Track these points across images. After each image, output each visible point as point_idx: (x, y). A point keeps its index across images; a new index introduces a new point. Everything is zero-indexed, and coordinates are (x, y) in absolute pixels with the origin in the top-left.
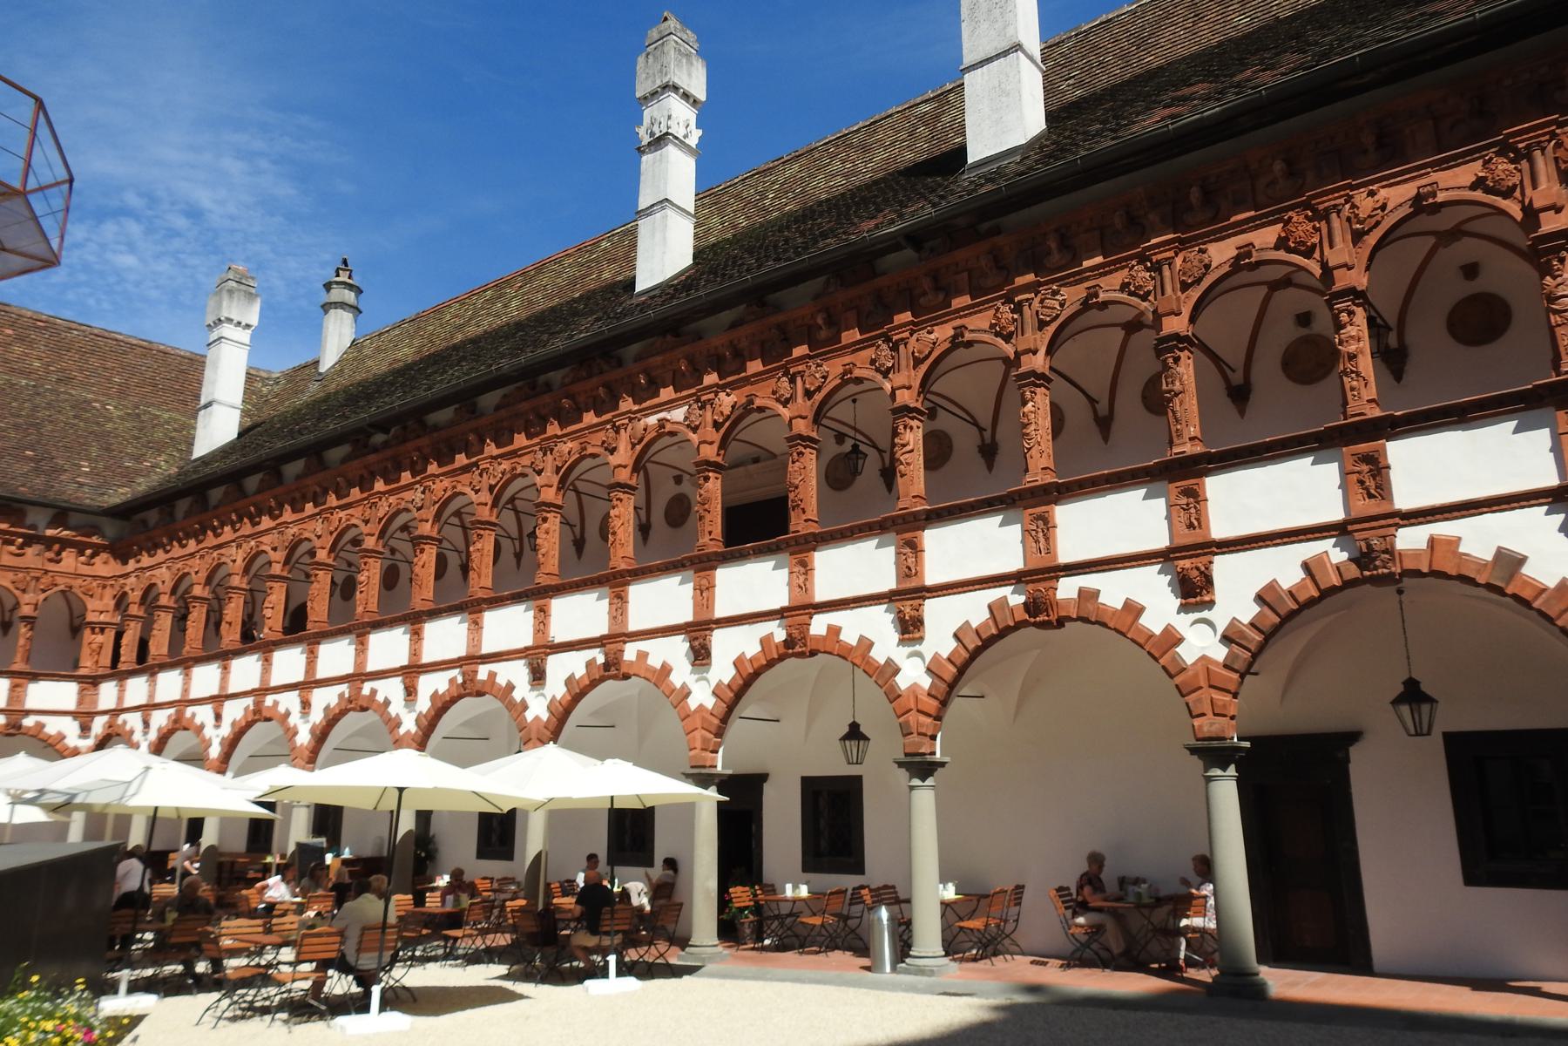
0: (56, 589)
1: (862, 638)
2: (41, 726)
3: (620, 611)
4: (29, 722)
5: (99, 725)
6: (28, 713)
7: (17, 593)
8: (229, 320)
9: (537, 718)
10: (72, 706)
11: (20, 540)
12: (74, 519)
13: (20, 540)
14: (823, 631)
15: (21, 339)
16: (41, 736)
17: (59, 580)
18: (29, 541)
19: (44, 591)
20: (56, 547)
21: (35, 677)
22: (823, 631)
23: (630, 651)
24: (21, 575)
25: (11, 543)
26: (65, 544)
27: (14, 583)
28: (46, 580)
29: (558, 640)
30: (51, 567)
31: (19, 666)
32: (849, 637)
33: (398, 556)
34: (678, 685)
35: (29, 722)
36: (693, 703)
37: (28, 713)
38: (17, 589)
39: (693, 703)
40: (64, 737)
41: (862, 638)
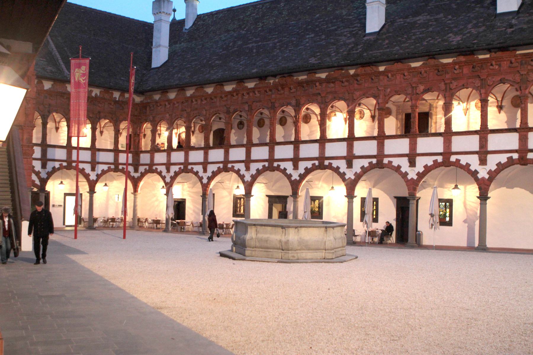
1: (467, 163)
3: (381, 148)
5: (142, 169)
8: (163, 12)
9: (350, 178)
14: (454, 160)
22: (454, 160)
23: (386, 161)
25: (111, 104)
29: (357, 154)
32: (463, 162)
33: (263, 116)
34: (404, 172)
36: (409, 177)
39: (409, 177)
41: (467, 163)
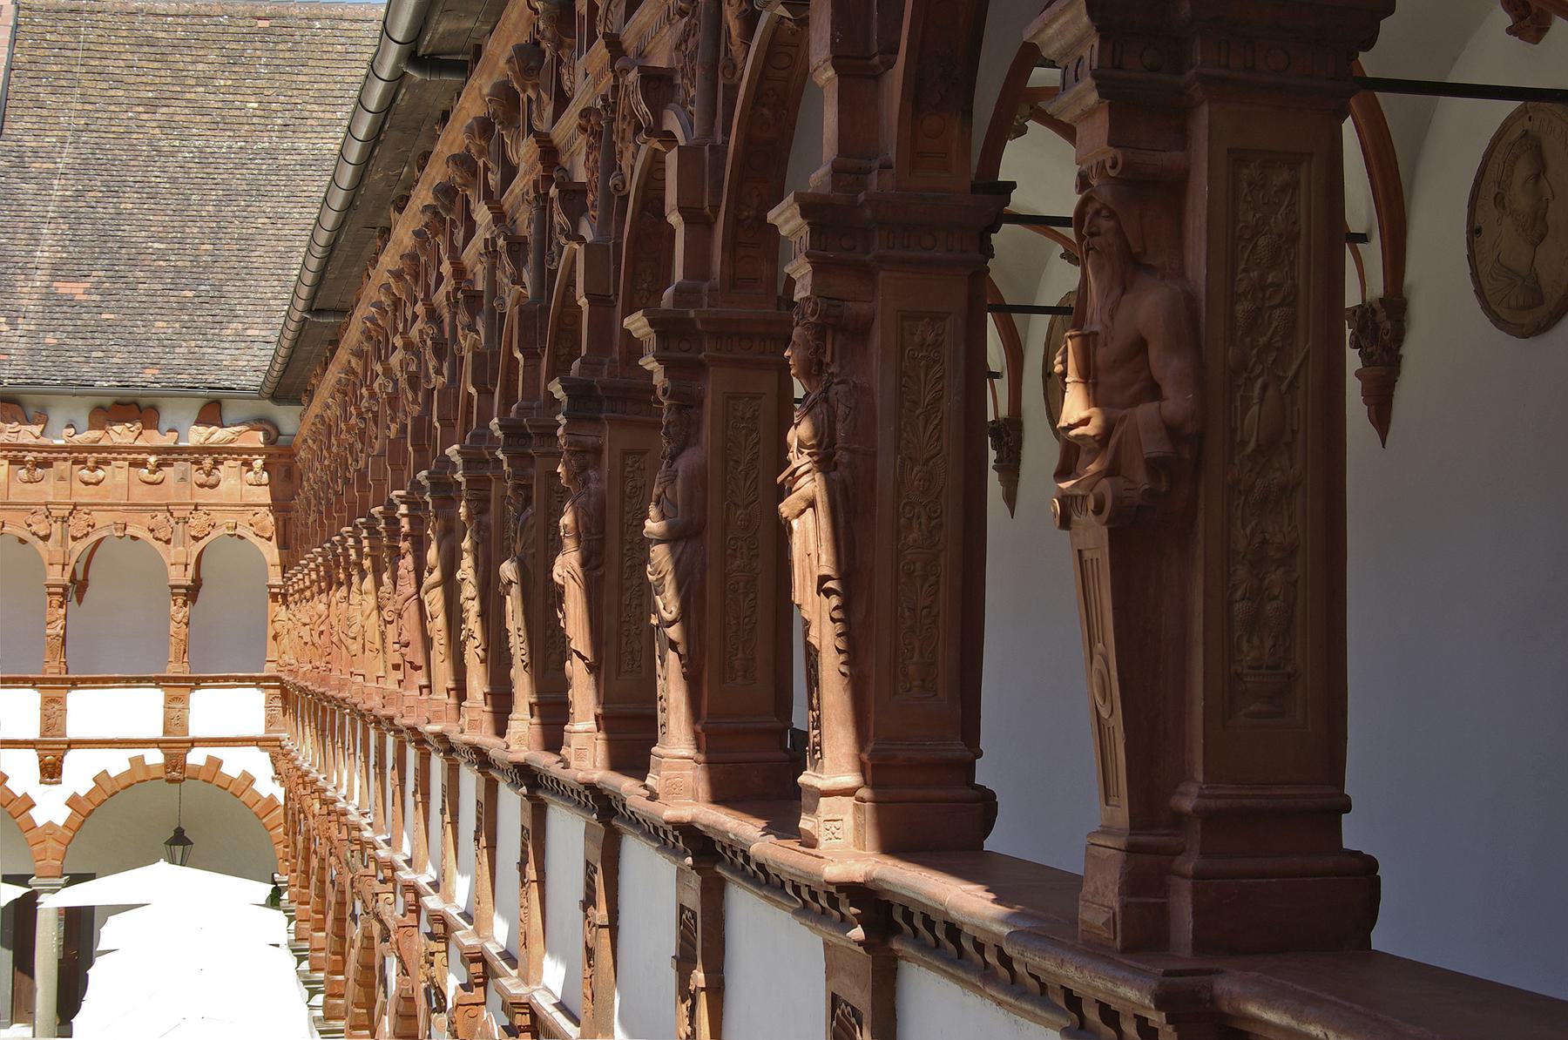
0: (214, 534)
2: (215, 764)
4: (196, 757)
6: (194, 743)
7: (159, 545)
10: (258, 730)
11: (152, 459)
12: (231, 411)
13: (152, 459)
15: (233, 60)
16: (217, 781)
17: (217, 517)
18: (168, 455)
19: (196, 539)
20: (208, 462)
21: (197, 683)
24: (160, 516)
25: (143, 464)
26: (218, 454)
27: (152, 531)
28: (198, 521)
30: (204, 496)
31: (174, 669)
35: (196, 757)
37: (194, 743)
38: (157, 539)
40: (252, 781)
